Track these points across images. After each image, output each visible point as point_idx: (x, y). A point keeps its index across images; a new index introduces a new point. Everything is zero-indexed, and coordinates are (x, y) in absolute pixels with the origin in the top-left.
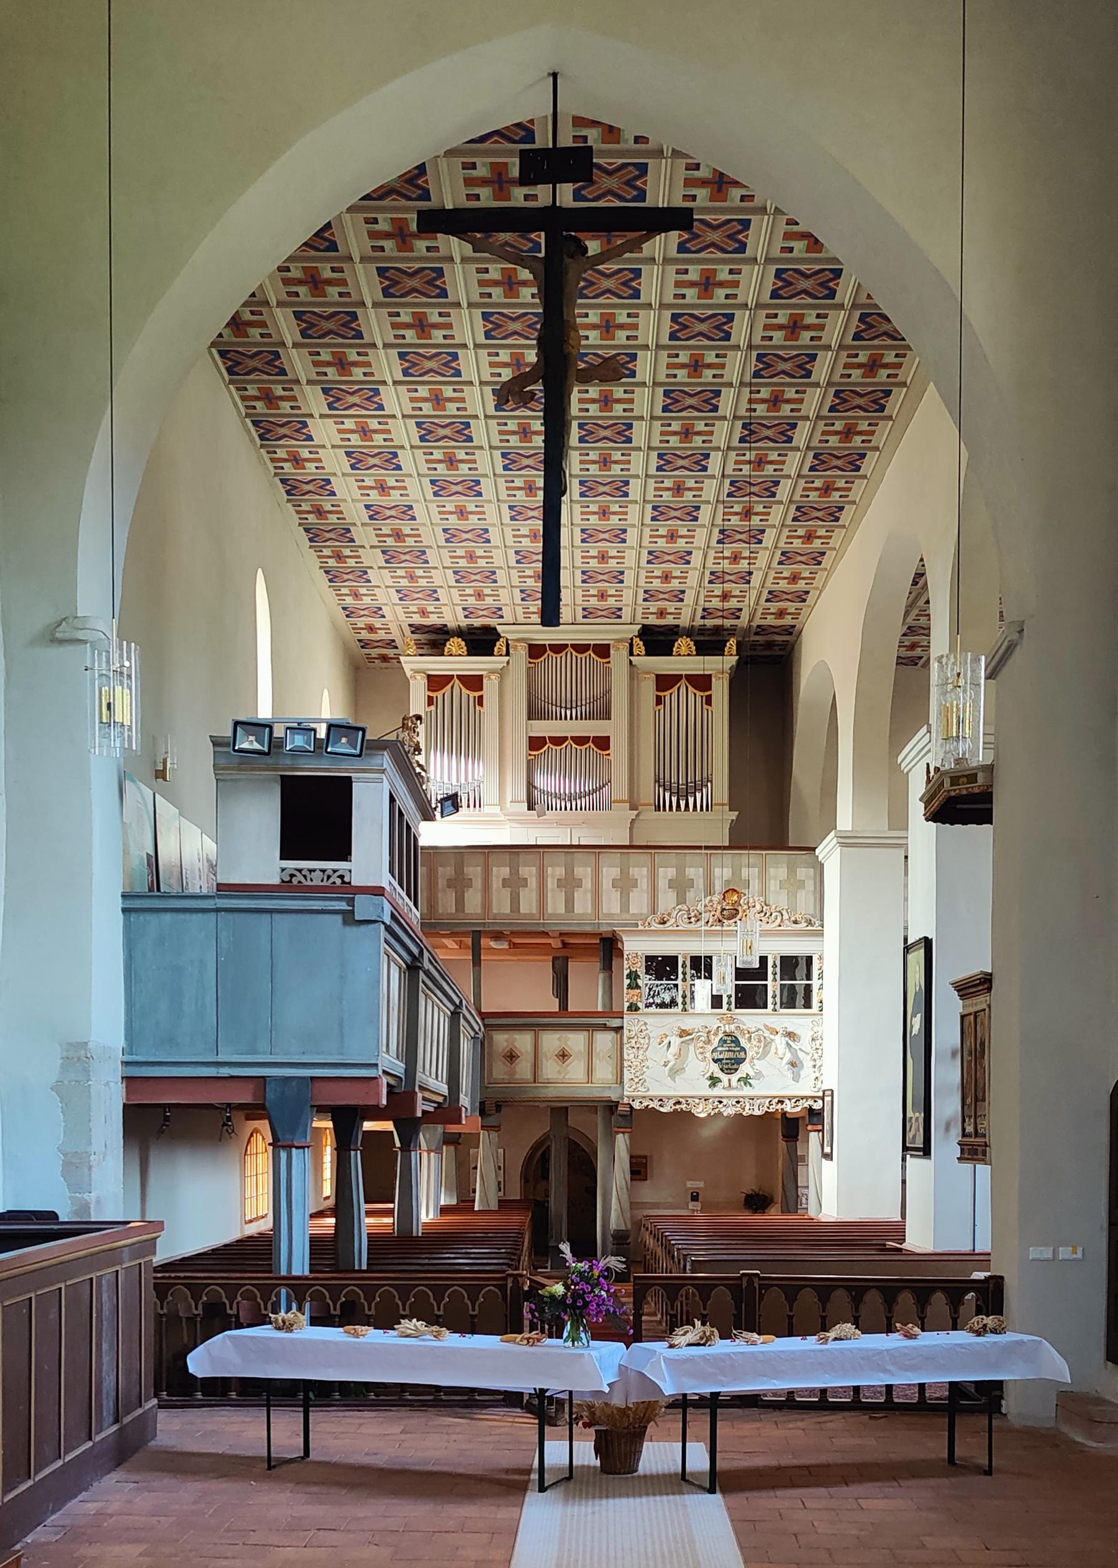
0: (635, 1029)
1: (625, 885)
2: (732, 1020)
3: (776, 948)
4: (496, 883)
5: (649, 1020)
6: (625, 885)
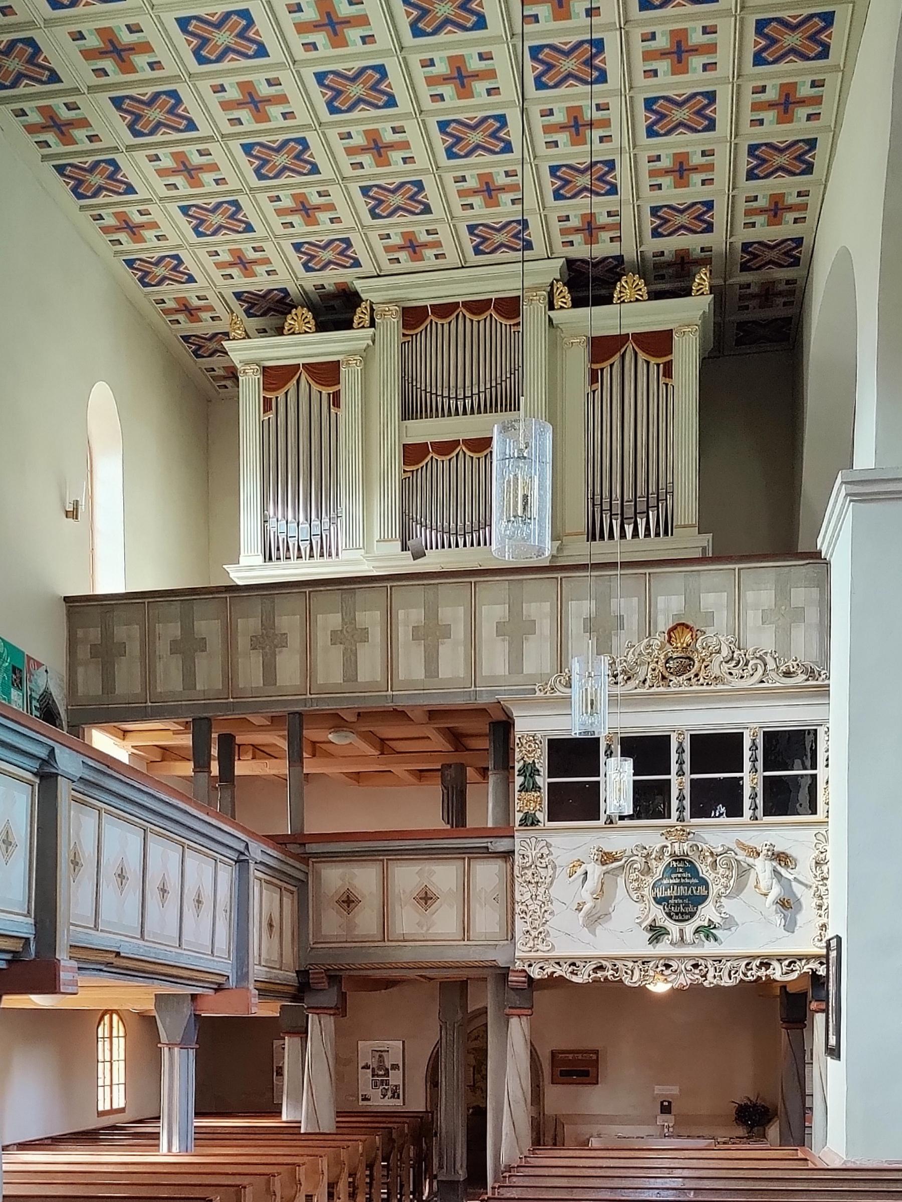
0: (532, 853)
1: (516, 631)
2: (685, 834)
3: (752, 719)
4: (322, 638)
5: (556, 840)
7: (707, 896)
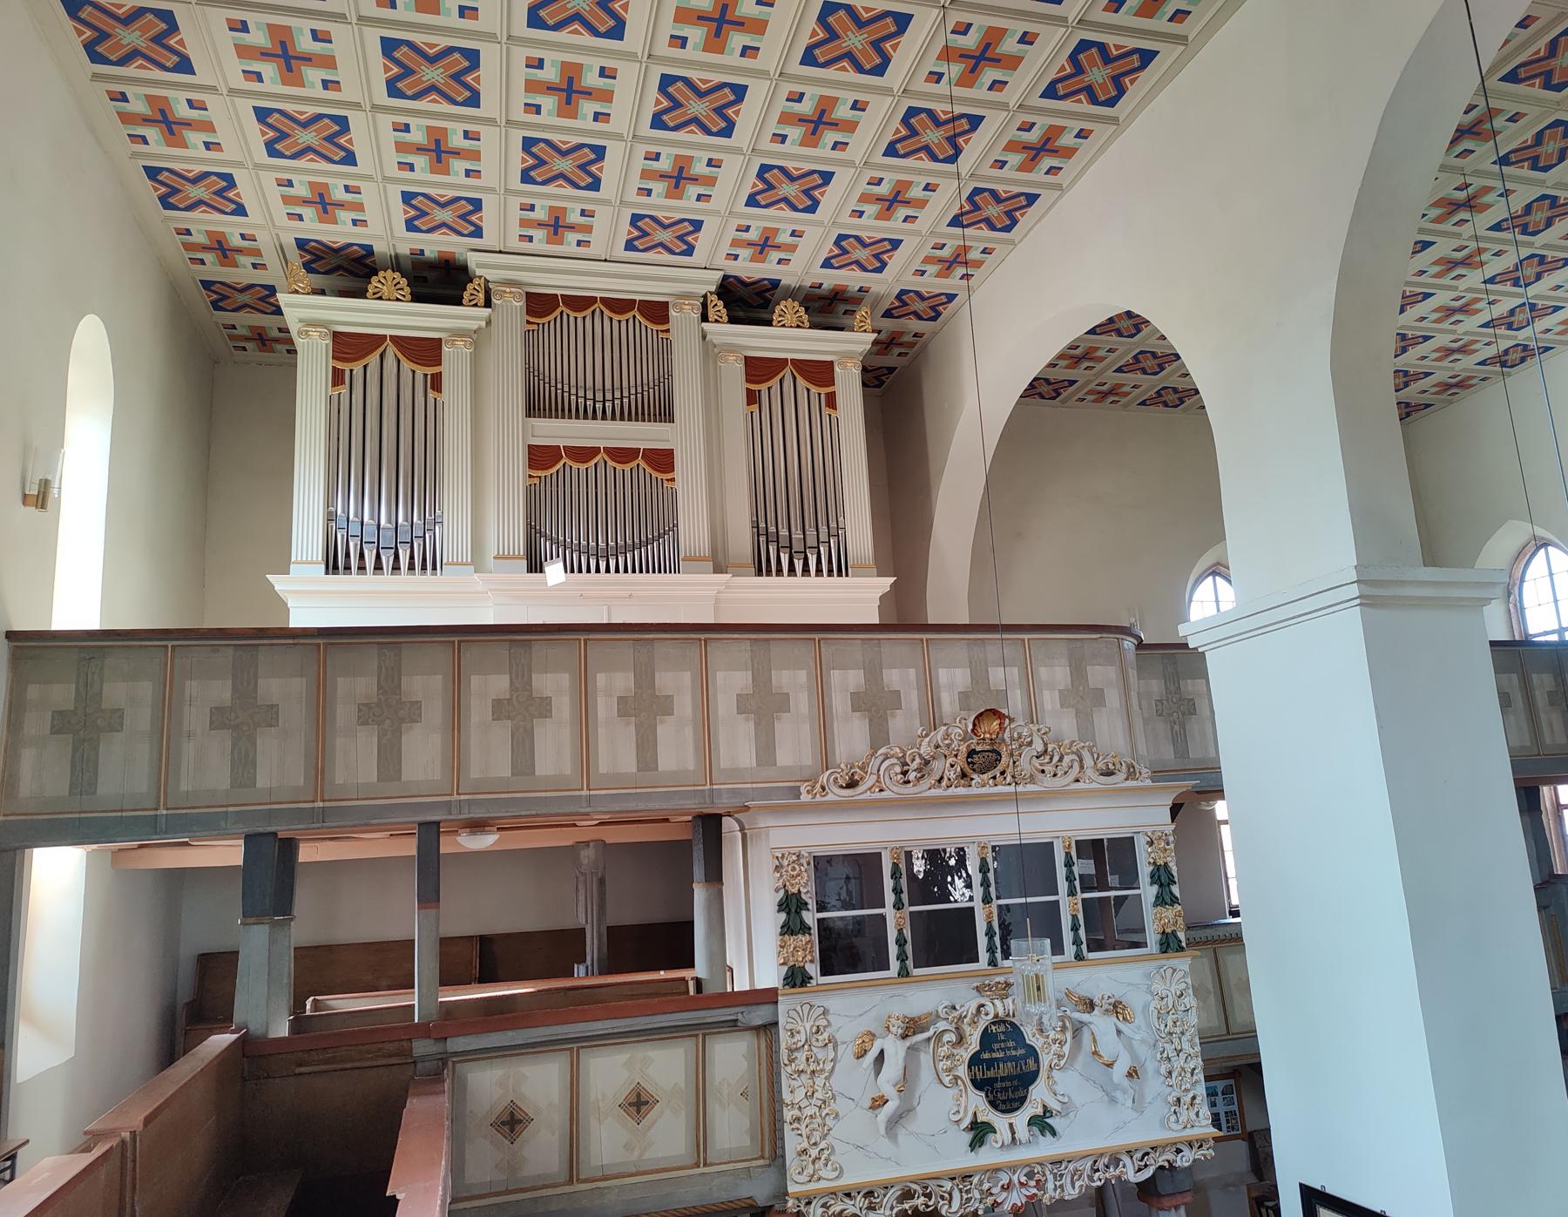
1: (764, 707)
4: (478, 711)
5: (835, 1003)
6: (764, 707)
7: (1038, 1071)
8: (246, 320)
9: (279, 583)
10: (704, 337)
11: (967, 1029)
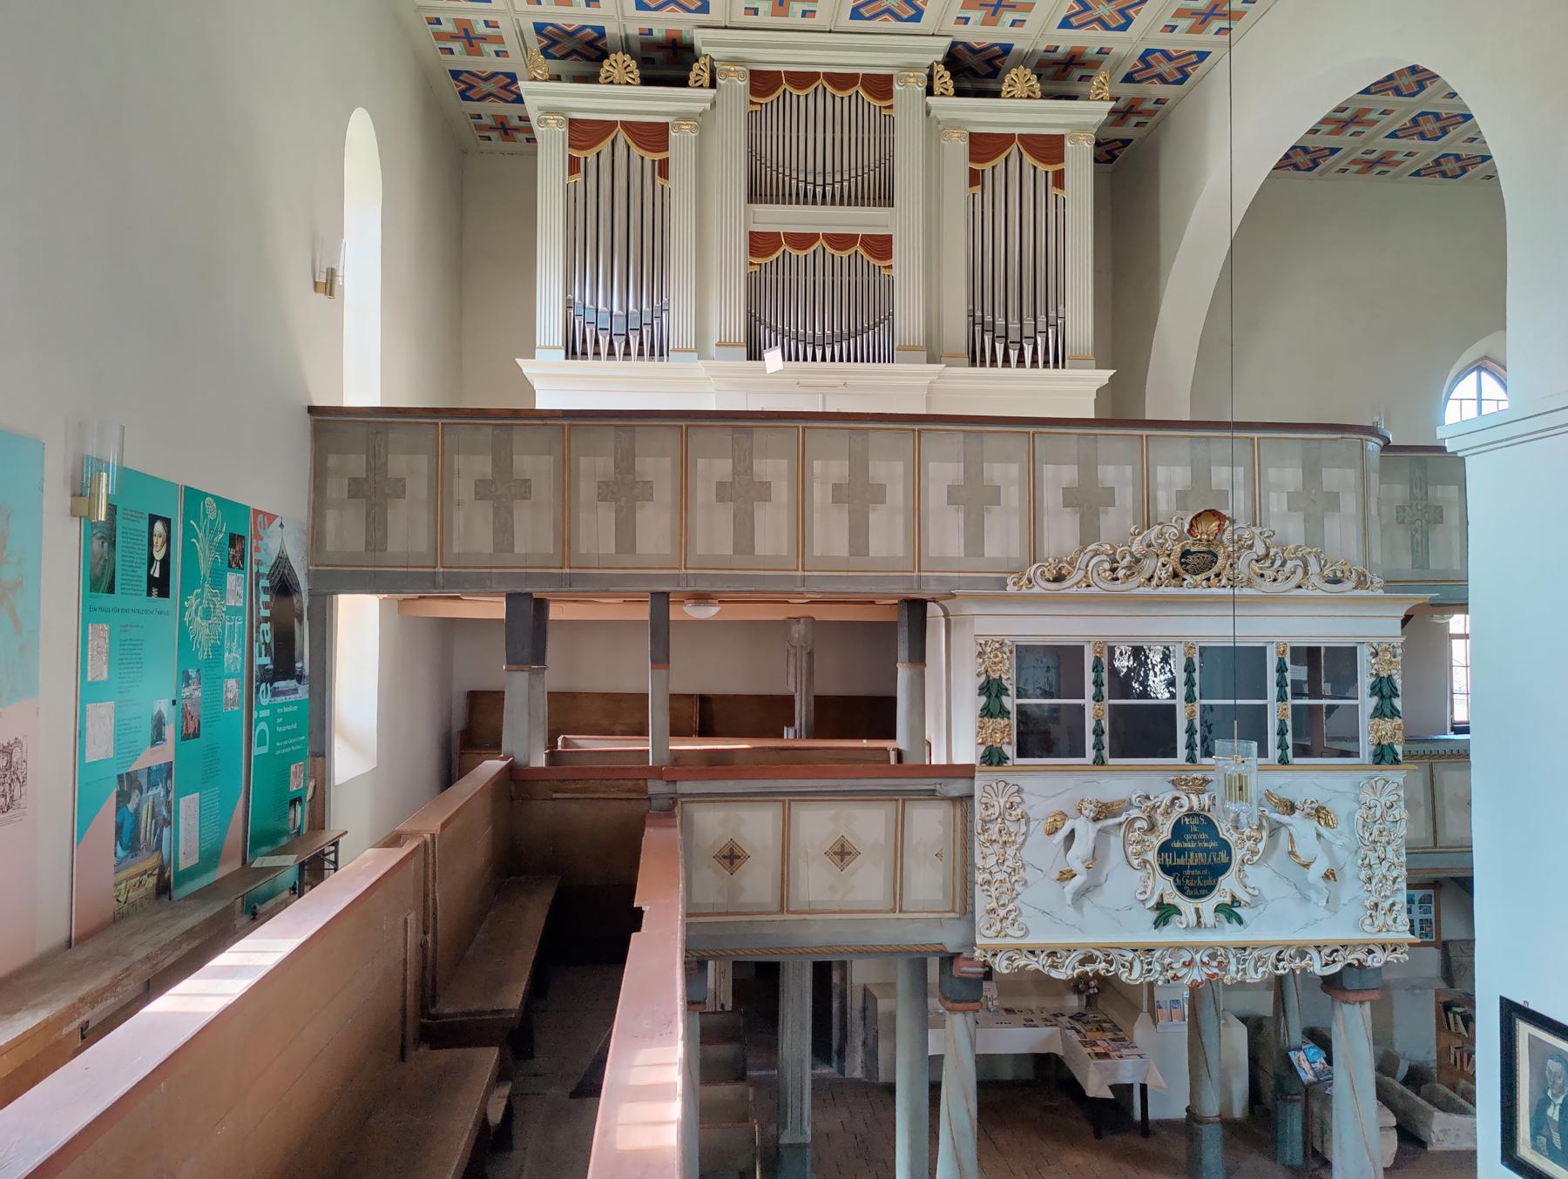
1: (975, 499)
4: (703, 492)
5: (1028, 783)
6: (975, 499)
8: (491, 109)
9: (526, 366)
10: (928, 113)
11: (1160, 819)
